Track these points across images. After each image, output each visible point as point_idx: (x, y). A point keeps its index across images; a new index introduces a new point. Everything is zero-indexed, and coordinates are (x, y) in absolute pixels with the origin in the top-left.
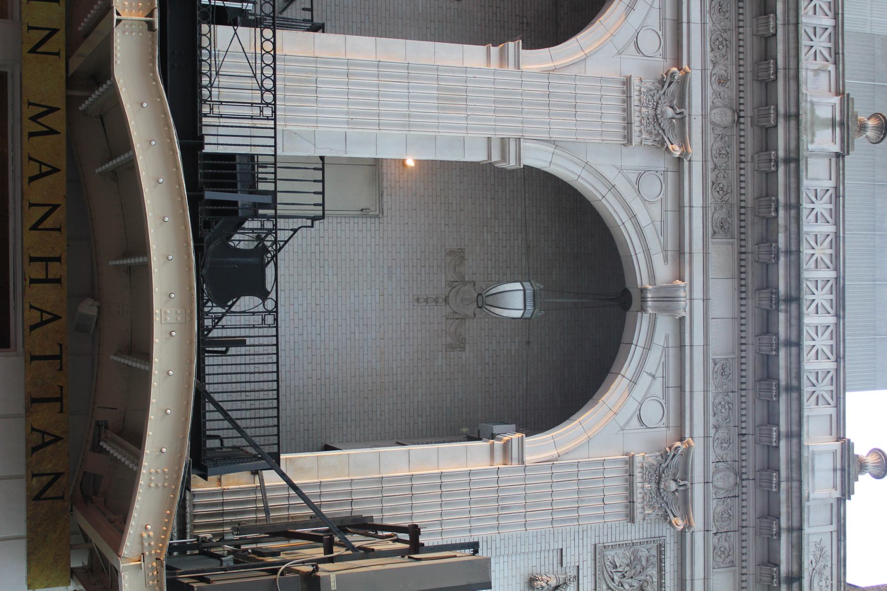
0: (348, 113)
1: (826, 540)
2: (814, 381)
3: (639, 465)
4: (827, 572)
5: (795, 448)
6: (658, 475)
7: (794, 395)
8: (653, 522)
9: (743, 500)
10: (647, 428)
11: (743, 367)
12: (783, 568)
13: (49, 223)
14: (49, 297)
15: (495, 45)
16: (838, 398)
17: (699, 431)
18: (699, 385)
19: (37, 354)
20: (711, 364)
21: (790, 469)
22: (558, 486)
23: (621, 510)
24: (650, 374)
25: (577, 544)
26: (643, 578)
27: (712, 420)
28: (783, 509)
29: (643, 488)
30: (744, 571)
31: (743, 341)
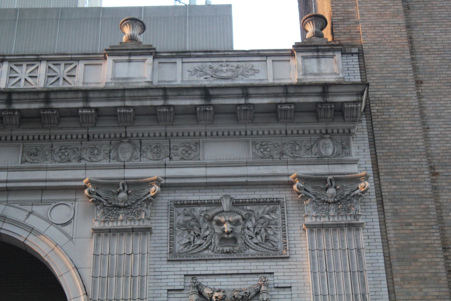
1: (188, 67)
2: (55, 79)
3: (102, 224)
4: (216, 66)
5: (97, 95)
6: (111, 208)
7: (52, 96)
8: (154, 211)
9: (143, 136)
10: (73, 218)
11: (31, 138)
12: (197, 102)
16: (72, 59)
17: (79, 174)
18: (41, 175)
20: (26, 165)
21: (114, 99)
22: (112, 294)
23: (139, 239)
24: (28, 216)
25: (166, 277)
26: (201, 219)
27: (74, 163)
28: (148, 103)
29: (122, 221)
30: (203, 134)
31: (9, 138)
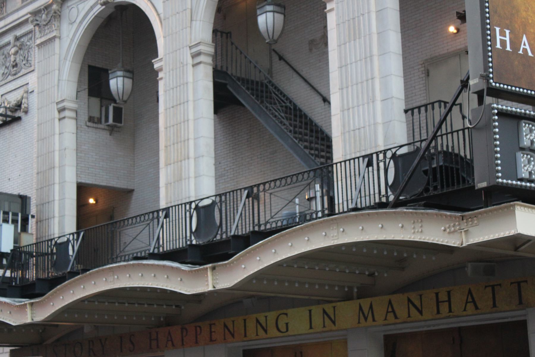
0: (368, 103)
13: (417, 303)
14: (459, 298)
15: (326, 8)
19: (492, 303)
